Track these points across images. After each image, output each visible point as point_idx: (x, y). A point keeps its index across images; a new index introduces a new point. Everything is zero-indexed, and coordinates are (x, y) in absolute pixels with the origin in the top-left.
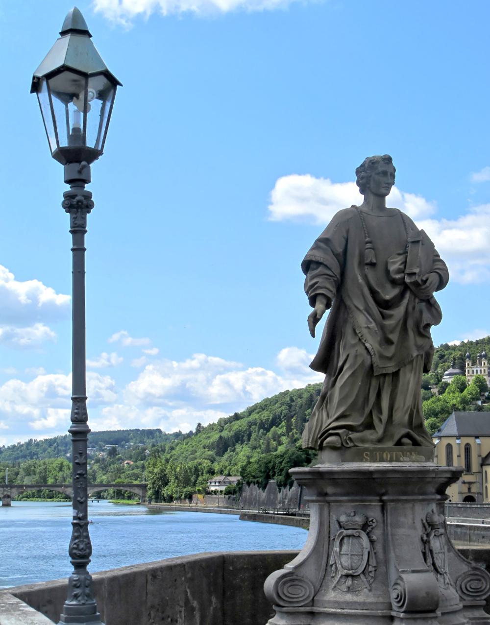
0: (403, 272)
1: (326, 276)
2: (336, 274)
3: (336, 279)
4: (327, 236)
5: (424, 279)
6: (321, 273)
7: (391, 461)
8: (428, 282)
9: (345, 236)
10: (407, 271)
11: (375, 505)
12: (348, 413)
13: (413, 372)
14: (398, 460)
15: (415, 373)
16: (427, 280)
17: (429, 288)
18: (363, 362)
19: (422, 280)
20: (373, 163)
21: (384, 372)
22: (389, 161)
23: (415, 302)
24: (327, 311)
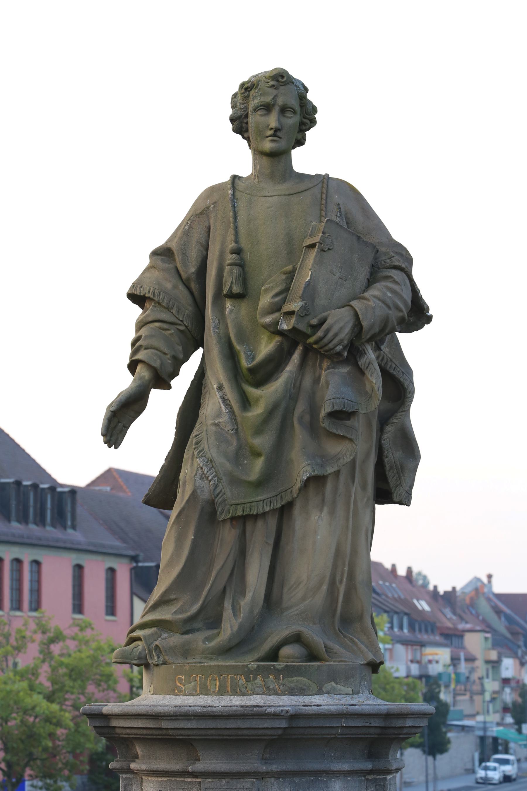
0: (279, 309)
1: (157, 324)
2: (181, 319)
3: (182, 328)
4: (169, 245)
5: (314, 322)
6: (150, 319)
7: (222, 692)
8: (325, 327)
9: (203, 241)
10: (286, 308)
11: (190, 783)
12: (172, 597)
13: (326, 510)
14: (236, 692)
15: (332, 512)
16: (322, 322)
17: (326, 340)
18: (194, 494)
19: (312, 327)
20: (246, 89)
21: (239, 513)
22: (278, 81)
23: (321, 368)
24: (155, 394)
